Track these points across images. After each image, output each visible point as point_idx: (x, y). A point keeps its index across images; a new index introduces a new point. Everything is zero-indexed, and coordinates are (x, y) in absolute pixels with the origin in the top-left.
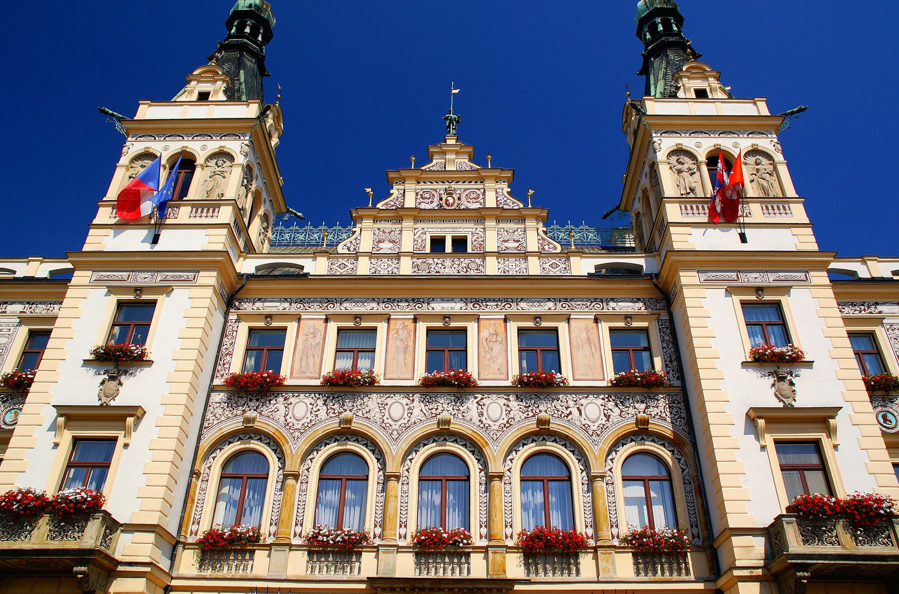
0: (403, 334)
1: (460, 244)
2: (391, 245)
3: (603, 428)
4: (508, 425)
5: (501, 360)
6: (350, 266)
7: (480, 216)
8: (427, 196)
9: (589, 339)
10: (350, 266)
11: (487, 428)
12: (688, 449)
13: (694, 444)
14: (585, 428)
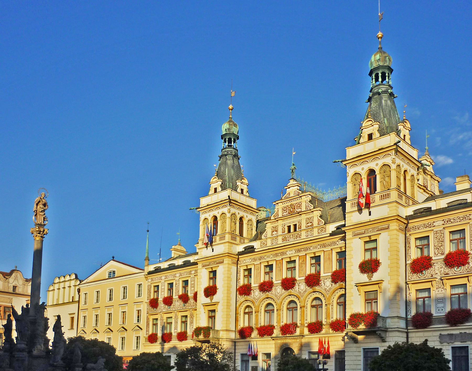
0: (279, 265)
3: (330, 289)
4: (305, 291)
9: (329, 258)
11: (300, 293)
14: (325, 289)
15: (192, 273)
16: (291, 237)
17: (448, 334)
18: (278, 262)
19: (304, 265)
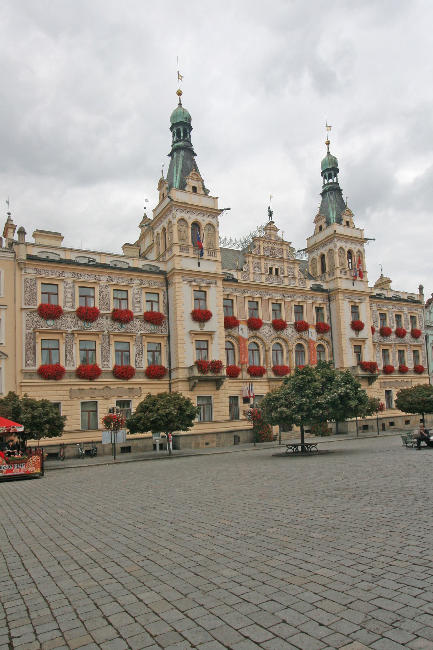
0: (266, 305)
1: (277, 270)
2: (258, 269)
4: (293, 336)
5: (290, 316)
6: (248, 277)
7: (282, 260)
8: (266, 249)
9: (311, 310)
10: (248, 277)
11: (288, 337)
12: (331, 344)
13: (332, 343)
15: (135, 282)
16: (275, 279)
17: (384, 382)
18: (264, 301)
19: (289, 311)
